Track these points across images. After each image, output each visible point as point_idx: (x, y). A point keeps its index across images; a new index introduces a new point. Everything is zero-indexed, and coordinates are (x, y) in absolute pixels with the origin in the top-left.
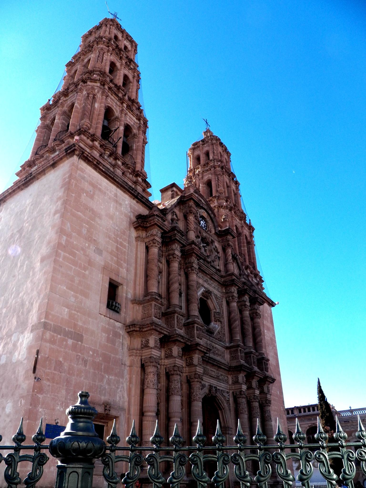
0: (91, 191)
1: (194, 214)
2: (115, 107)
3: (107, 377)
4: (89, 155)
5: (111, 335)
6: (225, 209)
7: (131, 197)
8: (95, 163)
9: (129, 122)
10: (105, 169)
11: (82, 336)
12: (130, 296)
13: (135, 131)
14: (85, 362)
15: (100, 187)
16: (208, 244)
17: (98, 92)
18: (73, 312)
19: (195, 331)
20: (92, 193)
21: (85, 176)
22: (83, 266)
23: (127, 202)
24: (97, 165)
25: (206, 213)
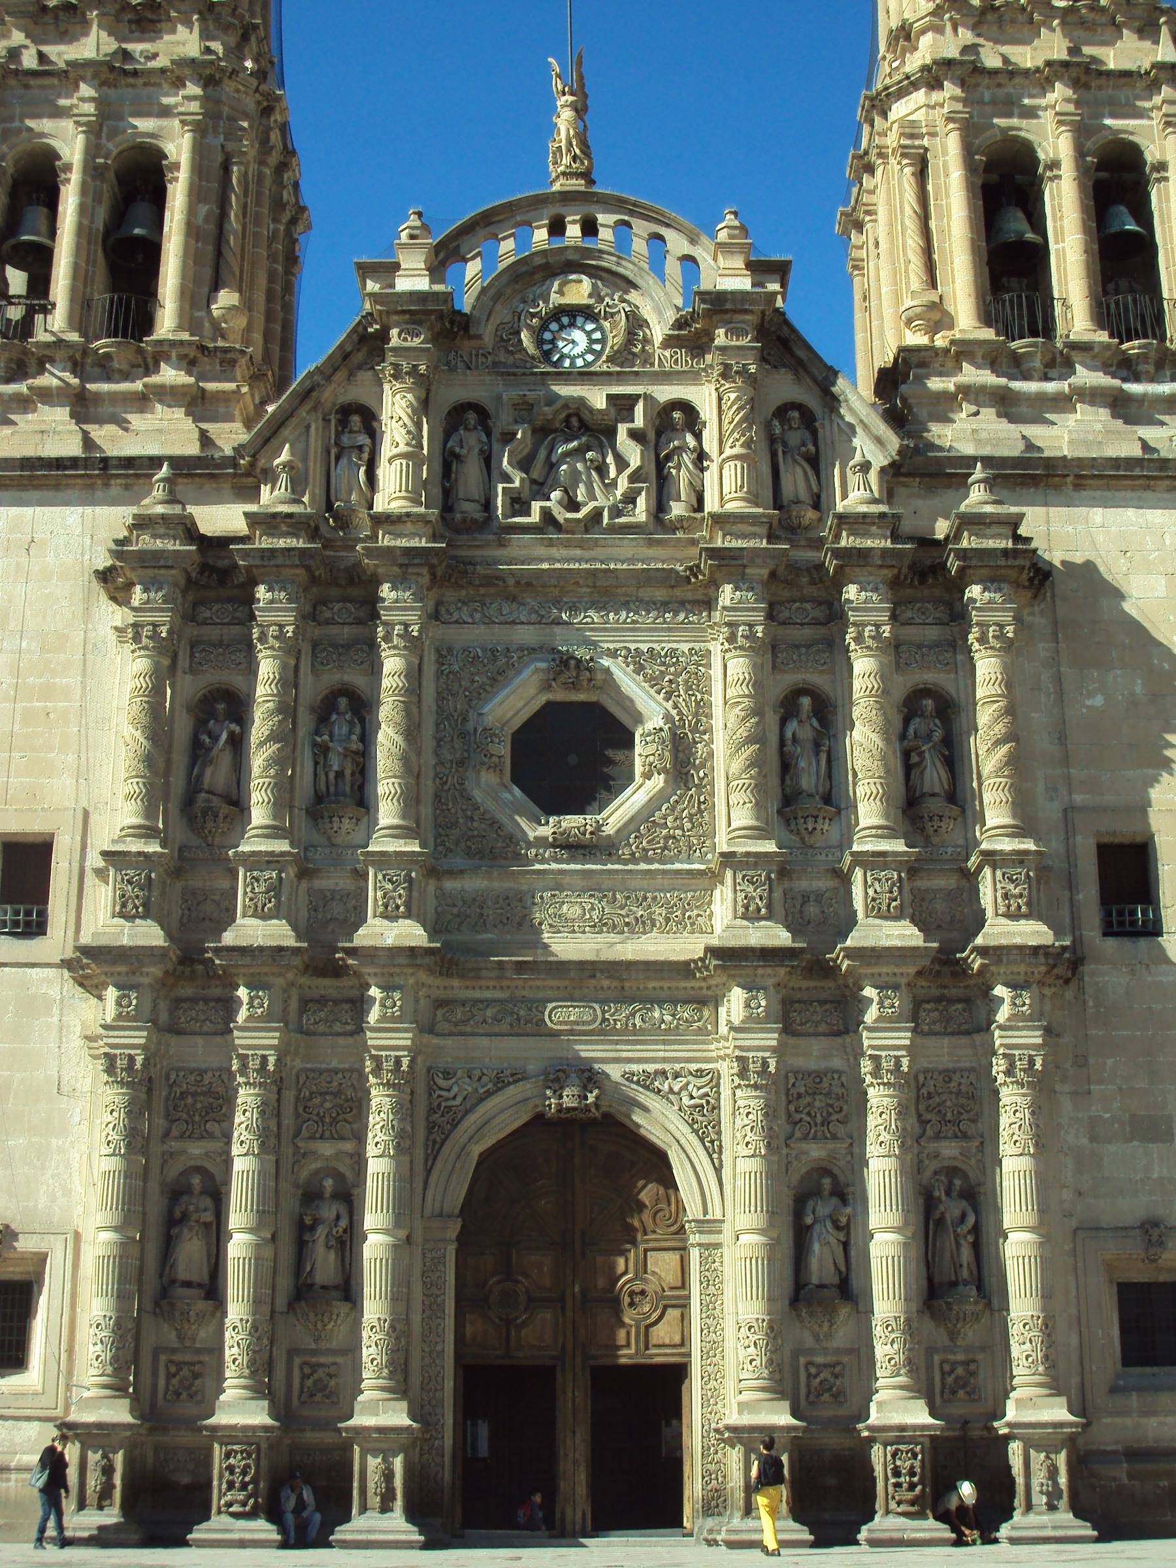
7: (92, 487)
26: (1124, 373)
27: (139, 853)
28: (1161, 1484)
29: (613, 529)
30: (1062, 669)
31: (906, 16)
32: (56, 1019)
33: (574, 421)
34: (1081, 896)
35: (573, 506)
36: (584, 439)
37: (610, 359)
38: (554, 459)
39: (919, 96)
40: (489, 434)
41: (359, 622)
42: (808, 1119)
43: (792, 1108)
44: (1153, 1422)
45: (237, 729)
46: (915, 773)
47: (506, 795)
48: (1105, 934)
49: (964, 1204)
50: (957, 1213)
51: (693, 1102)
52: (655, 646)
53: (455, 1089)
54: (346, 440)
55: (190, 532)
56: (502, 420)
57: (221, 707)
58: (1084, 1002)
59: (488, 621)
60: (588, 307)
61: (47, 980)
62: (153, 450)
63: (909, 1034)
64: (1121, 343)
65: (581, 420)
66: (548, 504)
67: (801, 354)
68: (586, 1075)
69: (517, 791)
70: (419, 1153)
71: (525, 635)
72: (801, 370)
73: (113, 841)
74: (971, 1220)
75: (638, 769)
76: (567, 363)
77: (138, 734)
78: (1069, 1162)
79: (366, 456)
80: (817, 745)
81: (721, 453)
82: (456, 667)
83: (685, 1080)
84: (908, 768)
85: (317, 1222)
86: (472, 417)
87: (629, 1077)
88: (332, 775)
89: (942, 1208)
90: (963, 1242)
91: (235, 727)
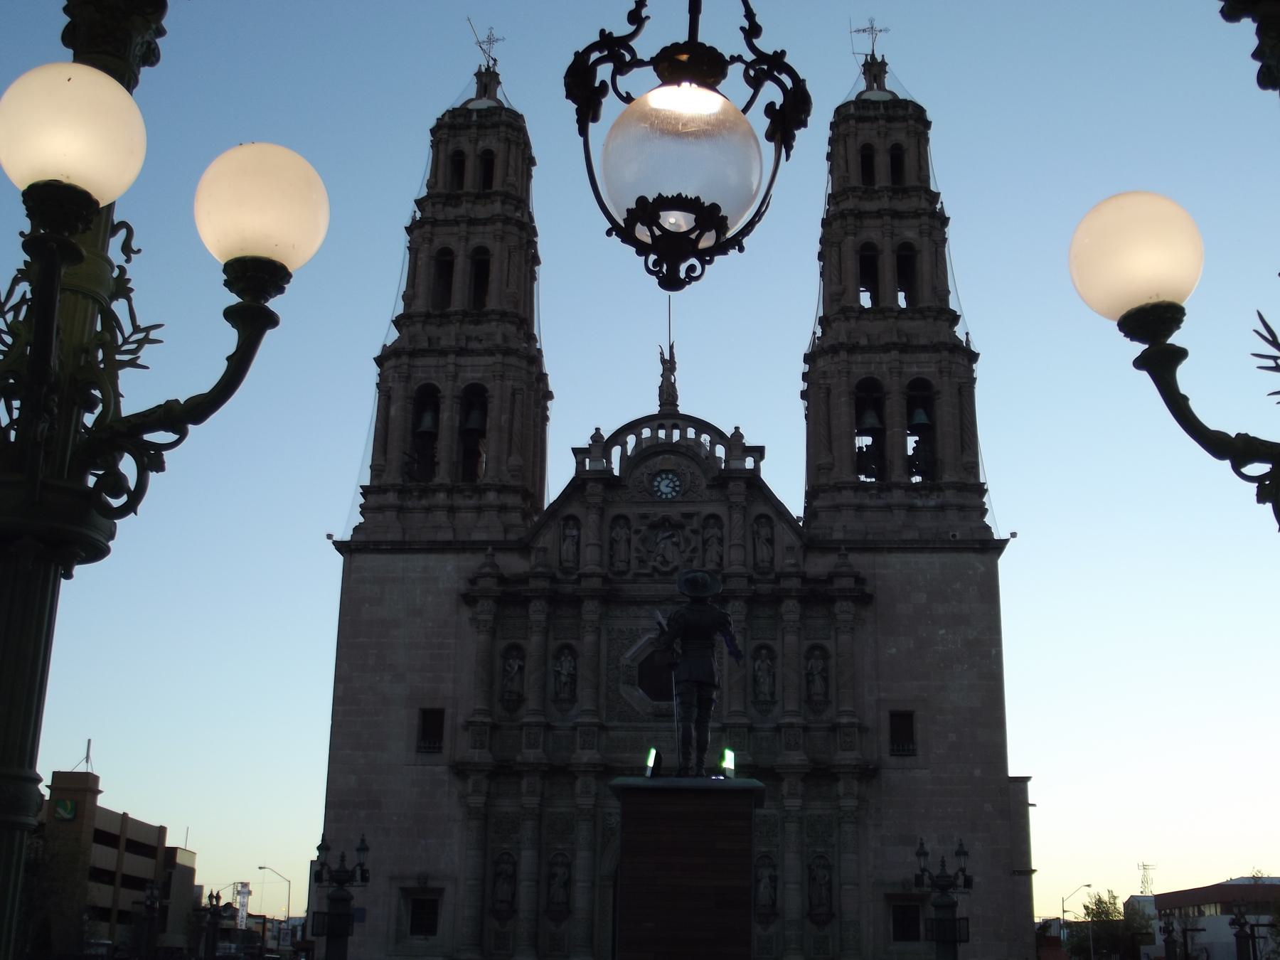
1: (594, 507)
8: (372, 547)
12: (461, 720)
13: (488, 386)
23: (449, 568)
27: (482, 722)
35: (665, 562)
37: (683, 495)
38: (658, 540)
40: (629, 529)
48: (892, 755)
54: (567, 532)
55: (502, 580)
66: (655, 564)
69: (641, 690)
74: (827, 879)
76: (664, 496)
84: (808, 682)
91: (521, 663)
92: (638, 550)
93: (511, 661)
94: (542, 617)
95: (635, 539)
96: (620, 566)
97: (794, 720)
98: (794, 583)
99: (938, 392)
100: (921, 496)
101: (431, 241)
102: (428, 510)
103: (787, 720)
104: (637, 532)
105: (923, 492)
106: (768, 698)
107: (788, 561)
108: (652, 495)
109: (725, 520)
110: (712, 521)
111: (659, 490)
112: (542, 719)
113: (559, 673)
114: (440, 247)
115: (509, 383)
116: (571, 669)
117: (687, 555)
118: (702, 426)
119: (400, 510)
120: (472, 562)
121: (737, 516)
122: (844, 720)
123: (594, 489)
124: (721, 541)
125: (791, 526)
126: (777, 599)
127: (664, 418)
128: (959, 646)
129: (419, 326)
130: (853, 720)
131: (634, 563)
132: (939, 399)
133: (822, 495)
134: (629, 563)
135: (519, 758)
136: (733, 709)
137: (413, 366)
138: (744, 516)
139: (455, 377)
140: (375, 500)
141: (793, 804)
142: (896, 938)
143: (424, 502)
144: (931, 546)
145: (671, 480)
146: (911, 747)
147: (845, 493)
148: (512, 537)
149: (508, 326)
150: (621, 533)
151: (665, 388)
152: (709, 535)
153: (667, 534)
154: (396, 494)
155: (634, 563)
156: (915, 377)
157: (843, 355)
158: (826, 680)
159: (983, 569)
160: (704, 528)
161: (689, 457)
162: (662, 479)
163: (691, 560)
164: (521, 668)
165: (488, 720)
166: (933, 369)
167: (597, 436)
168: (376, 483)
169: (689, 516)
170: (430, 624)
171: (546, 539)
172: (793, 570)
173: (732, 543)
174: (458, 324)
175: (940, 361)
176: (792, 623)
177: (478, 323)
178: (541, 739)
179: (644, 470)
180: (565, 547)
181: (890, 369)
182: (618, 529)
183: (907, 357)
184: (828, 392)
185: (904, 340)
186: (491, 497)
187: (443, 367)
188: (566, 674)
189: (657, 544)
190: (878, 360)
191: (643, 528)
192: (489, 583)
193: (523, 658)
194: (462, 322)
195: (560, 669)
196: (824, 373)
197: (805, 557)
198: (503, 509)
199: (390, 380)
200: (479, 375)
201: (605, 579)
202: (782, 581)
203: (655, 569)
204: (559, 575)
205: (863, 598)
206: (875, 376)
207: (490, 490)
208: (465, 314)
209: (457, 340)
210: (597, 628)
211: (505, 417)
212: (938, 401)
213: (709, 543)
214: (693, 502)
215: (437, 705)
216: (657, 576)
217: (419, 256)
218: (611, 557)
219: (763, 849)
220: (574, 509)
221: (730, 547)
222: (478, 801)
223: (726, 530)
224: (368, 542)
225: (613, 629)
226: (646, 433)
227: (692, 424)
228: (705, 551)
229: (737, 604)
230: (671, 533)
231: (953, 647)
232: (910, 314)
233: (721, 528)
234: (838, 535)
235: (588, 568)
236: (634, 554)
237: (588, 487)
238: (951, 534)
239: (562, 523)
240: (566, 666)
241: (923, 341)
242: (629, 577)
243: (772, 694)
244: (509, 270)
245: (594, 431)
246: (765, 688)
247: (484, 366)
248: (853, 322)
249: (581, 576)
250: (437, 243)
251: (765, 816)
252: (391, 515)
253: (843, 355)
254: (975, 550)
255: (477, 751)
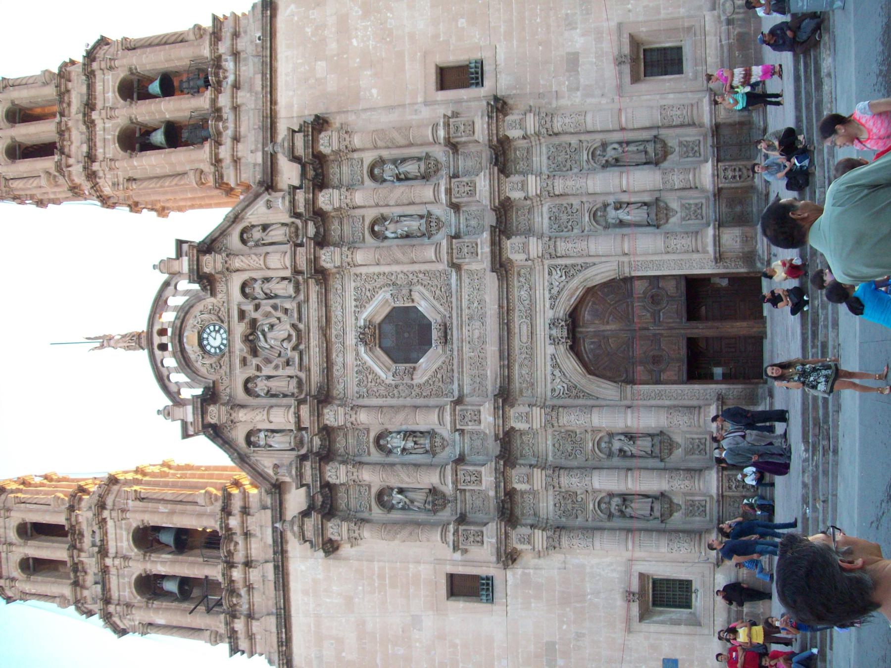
0: (332, 644)
1: (230, 415)
2: (127, 580)
3: (589, 597)
4: (281, 662)
5: (530, 592)
6: (100, 187)
8: (284, 648)
9: (128, 540)
10: (281, 629)
11: (547, 643)
12: (458, 556)
13: (134, 525)
14: (579, 636)
15: (312, 626)
16: (253, 323)
17: (133, 620)
18: (520, 660)
19: (470, 427)
20: (333, 642)
21: (313, 655)
22: (451, 650)
23: (303, 568)
24: (284, 644)
25: (185, 334)
26: (224, 84)
27: (454, 534)
28: (737, 55)
29: (300, 319)
30: (360, 108)
31: (66, 189)
32: (531, 571)
33: (251, 338)
34: (465, 97)
35: (290, 336)
36: (259, 333)
37: (222, 322)
38: (268, 347)
39: (101, 182)
40: (258, 377)
41: (346, 435)
42: (570, 223)
43: (565, 230)
44: (709, 59)
45: (396, 490)
46: (410, 176)
47: (424, 365)
48: (483, 86)
49: (609, 149)
50: (613, 152)
51: (564, 277)
52: (353, 297)
53: (559, 387)
54: (262, 443)
55: (305, 514)
56: (251, 372)
57: (386, 498)
58: (514, 94)
59: (344, 375)
60: (199, 333)
61: (514, 575)
62: (269, 531)
63: (530, 176)
64: (210, 85)
65: (251, 334)
66: (289, 349)
67: (217, 234)
68: (552, 326)
69: (421, 361)
70: (590, 402)
71: (350, 358)
72: (225, 233)
73: (449, 546)
74: (616, 146)
75: (411, 305)
76: (225, 342)
77: (398, 536)
78: (589, 100)
79: (269, 434)
80: (397, 222)
81: (262, 269)
82: (365, 390)
83: (554, 280)
84: (407, 179)
85: (621, 450)
86: (250, 385)
87: (552, 307)
88: (416, 446)
89: (610, 159)
90: (626, 149)
92: (276, 367)
93: (394, 502)
94: (343, 468)
95: (267, 371)
96: (292, 387)
97: (442, 189)
98: (300, 196)
99: (130, 69)
100: (225, 78)
101: (13, 579)
102: (250, 588)
103: (443, 196)
104: (258, 368)
105: (221, 75)
106: (423, 221)
107: (280, 206)
108: (225, 352)
109: (245, 276)
110: (247, 290)
111: (219, 347)
112: (449, 468)
113: (404, 450)
114: (19, 570)
115: (130, 502)
116: (398, 436)
117: (279, 314)
118: (159, 304)
119: (250, 616)
120: (294, 547)
121: (237, 263)
122: (441, 133)
123: (215, 414)
124: (267, 280)
125: (248, 206)
126: (319, 215)
127: (152, 344)
128: (369, 23)
129: (86, 593)
130: (442, 124)
131: (290, 371)
132: (136, 69)
133: (225, 180)
134: (291, 377)
135: (492, 493)
136: (434, 258)
137: (119, 600)
138: (238, 255)
139: (126, 558)
140: (243, 644)
141: (533, 184)
142: (680, 71)
143: (243, 592)
144: (269, 60)
145: (209, 334)
146: (473, 65)
147: (221, 156)
148: (268, 501)
149: (83, 504)
150: (261, 386)
151: (126, 345)
152: (261, 292)
153: (261, 337)
154: (236, 620)
155: (290, 371)
156: (117, 94)
157: (96, 167)
158: (404, 160)
159: (293, 7)
160: (256, 298)
161: (184, 317)
162: (209, 344)
163: (286, 311)
164: (401, 491)
165: (451, 528)
166: (110, 77)
167: (167, 413)
168: (227, 640)
169: (242, 314)
170: (360, 588)
171: (266, 463)
172: (287, 198)
173: (263, 266)
174: (83, 554)
175: (101, 69)
176: (342, 197)
177: (81, 534)
178: (471, 468)
179: (199, 363)
180: (276, 446)
181: (107, 118)
182: (257, 389)
183: (99, 104)
184: (130, 180)
185: (82, 110)
186: (234, 522)
187: (117, 569)
188: (404, 442)
189: (271, 347)
190: (102, 132)
191: (255, 361)
192: (310, 524)
193: (392, 489)
194: (81, 550)
195: (399, 449)
196: (114, 184)
197: (281, 190)
198: (245, 511)
199: (133, 623)
200: (124, 533)
201: (300, 402)
202: (298, 211)
203: (294, 348)
204: (303, 451)
205: (320, 124)
206: (117, 134)
207: (227, 525)
208: (73, 547)
209: (93, 556)
210: (352, 409)
211: (162, 508)
212: (138, 70)
213: (268, 292)
214: (229, 310)
215: (443, 583)
216: (302, 347)
217: (28, 592)
218: (285, 396)
219: (587, 219)
220: (239, 435)
221: (269, 269)
222: (539, 537)
223: (254, 275)
224: (279, 652)
225: (357, 393)
226: (170, 362)
227: (158, 315)
228: (276, 296)
229: (323, 257)
230: (259, 333)
231: (370, 29)
232: (65, 105)
233: (255, 280)
234: (259, 158)
235: (292, 419)
236: (280, 372)
237: (212, 422)
238: (258, 41)
239: (252, 449)
240: (396, 442)
241: (84, 89)
242: (303, 375)
243: (421, 217)
244: (35, 504)
245: (161, 416)
246: (414, 225)
247: (116, 530)
248: (71, 161)
249: (300, 429)
250: (16, 573)
251: (550, 218)
252: (256, 626)
253: (96, 167)
254: (273, 16)
255: (485, 539)
